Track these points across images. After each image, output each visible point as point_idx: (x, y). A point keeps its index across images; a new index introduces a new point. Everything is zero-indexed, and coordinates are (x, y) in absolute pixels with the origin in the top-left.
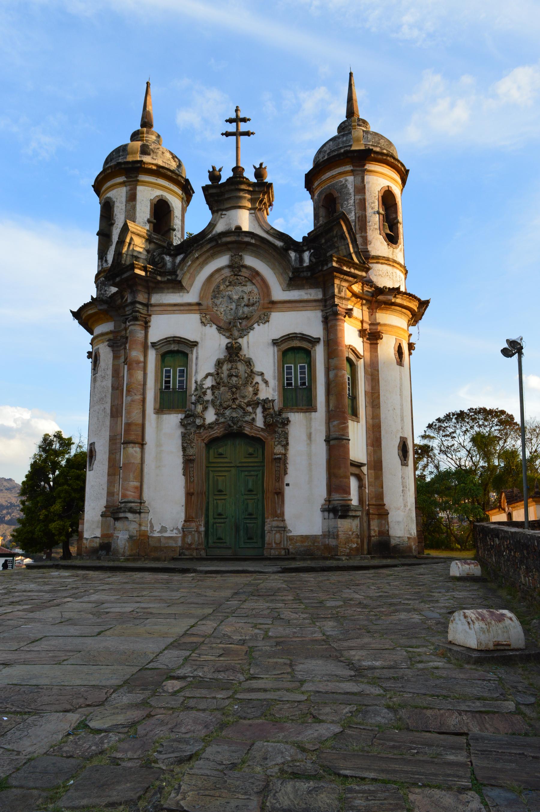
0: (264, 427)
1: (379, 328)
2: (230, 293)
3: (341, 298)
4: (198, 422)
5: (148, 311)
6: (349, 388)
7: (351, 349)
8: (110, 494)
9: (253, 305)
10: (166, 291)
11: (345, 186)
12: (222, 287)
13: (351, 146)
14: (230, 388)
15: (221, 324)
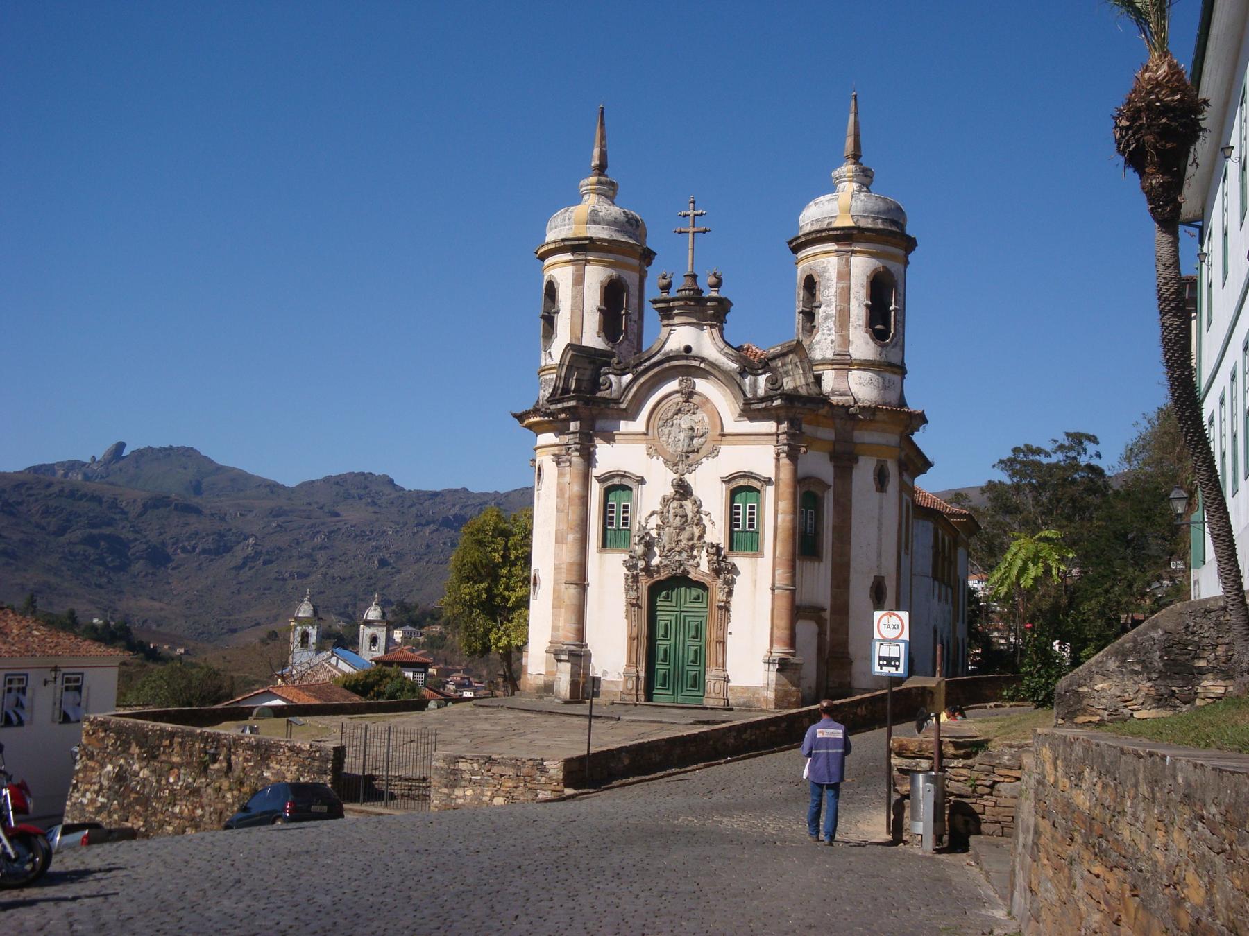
8: (555, 628)
11: (825, 270)
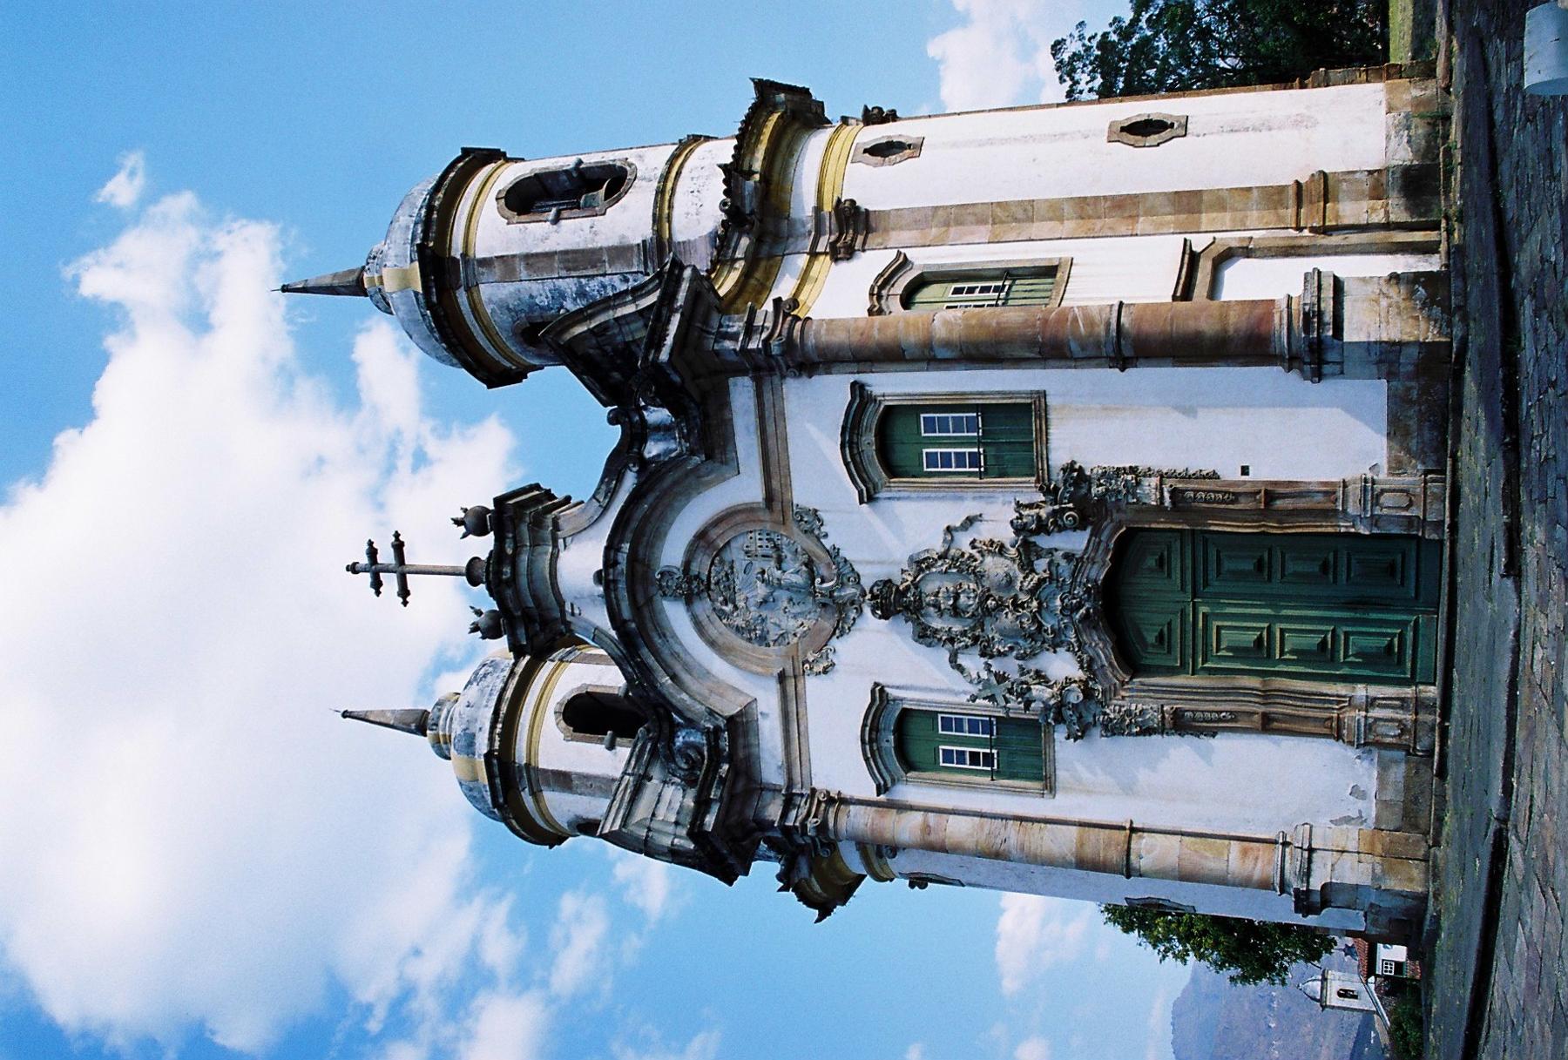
0: (1089, 530)
1: (828, 208)
2: (752, 601)
3: (750, 330)
4: (1075, 696)
5: (802, 795)
6: (985, 290)
7: (881, 288)
9: (777, 548)
10: (754, 750)
12: (739, 622)
13: (416, 294)
14: (988, 612)
15: (828, 625)
